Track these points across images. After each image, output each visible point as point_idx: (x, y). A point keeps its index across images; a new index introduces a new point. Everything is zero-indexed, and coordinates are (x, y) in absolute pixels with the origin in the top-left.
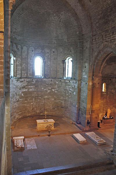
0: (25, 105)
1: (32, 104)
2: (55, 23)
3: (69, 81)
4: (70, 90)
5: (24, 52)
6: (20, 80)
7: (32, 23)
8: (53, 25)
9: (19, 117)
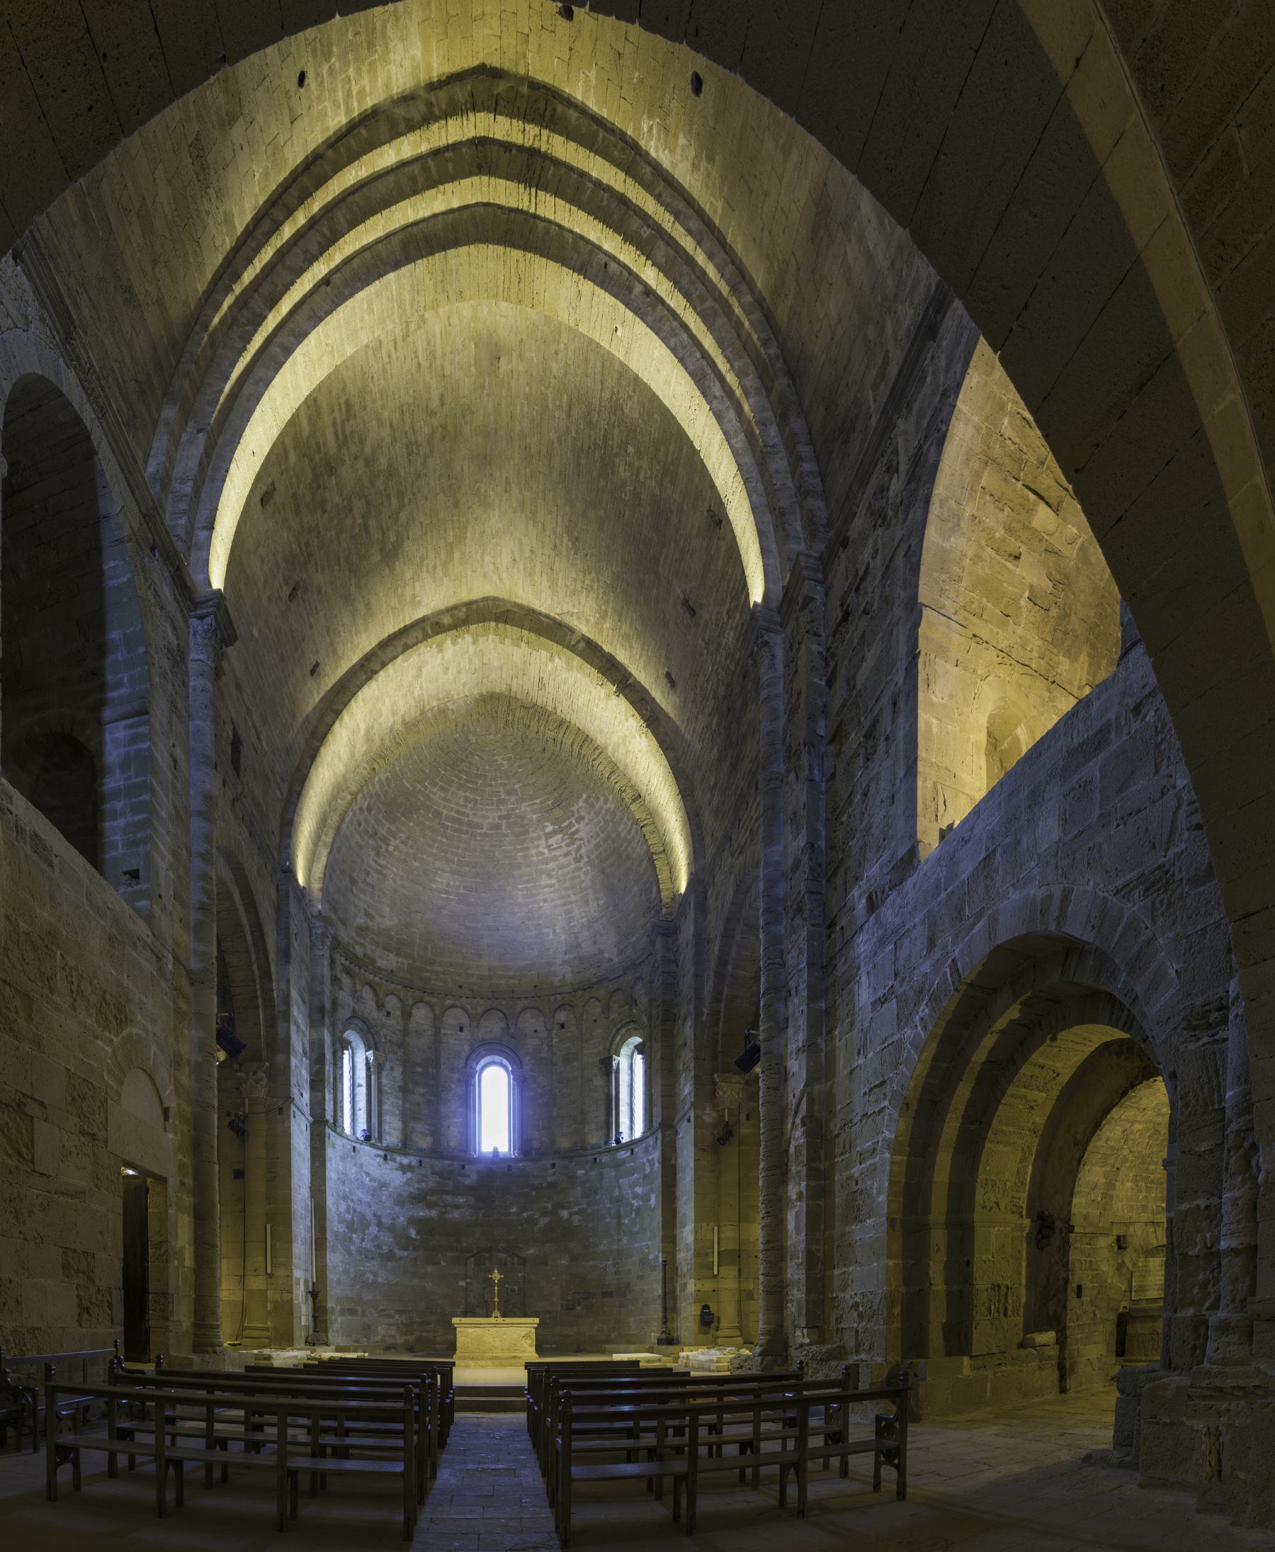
0: (428, 1285)
1: (462, 1284)
2: (557, 878)
3: (629, 1154)
4: (635, 1196)
5: (416, 1031)
6: (398, 1158)
7: (448, 885)
8: (551, 886)
9: (393, 1337)
